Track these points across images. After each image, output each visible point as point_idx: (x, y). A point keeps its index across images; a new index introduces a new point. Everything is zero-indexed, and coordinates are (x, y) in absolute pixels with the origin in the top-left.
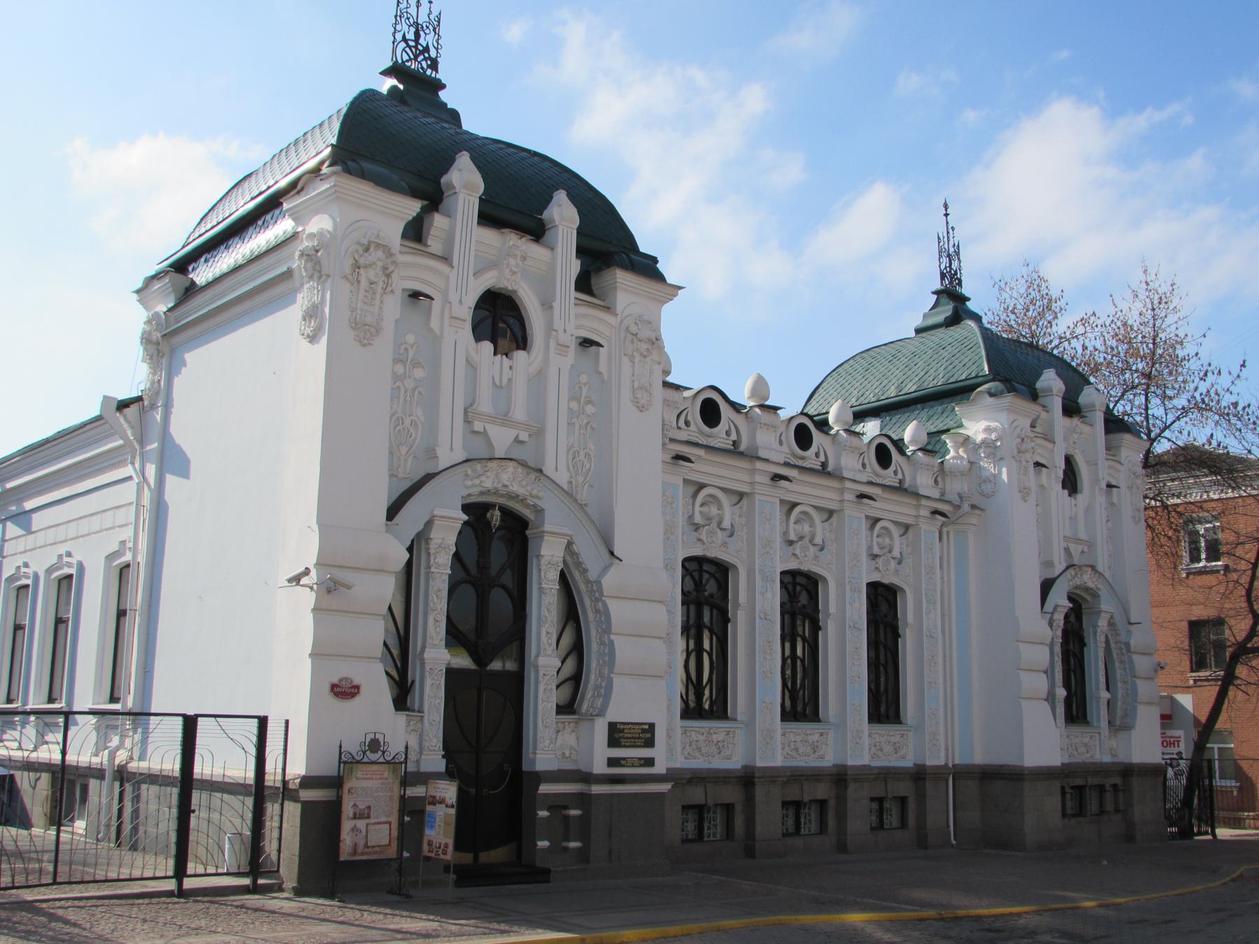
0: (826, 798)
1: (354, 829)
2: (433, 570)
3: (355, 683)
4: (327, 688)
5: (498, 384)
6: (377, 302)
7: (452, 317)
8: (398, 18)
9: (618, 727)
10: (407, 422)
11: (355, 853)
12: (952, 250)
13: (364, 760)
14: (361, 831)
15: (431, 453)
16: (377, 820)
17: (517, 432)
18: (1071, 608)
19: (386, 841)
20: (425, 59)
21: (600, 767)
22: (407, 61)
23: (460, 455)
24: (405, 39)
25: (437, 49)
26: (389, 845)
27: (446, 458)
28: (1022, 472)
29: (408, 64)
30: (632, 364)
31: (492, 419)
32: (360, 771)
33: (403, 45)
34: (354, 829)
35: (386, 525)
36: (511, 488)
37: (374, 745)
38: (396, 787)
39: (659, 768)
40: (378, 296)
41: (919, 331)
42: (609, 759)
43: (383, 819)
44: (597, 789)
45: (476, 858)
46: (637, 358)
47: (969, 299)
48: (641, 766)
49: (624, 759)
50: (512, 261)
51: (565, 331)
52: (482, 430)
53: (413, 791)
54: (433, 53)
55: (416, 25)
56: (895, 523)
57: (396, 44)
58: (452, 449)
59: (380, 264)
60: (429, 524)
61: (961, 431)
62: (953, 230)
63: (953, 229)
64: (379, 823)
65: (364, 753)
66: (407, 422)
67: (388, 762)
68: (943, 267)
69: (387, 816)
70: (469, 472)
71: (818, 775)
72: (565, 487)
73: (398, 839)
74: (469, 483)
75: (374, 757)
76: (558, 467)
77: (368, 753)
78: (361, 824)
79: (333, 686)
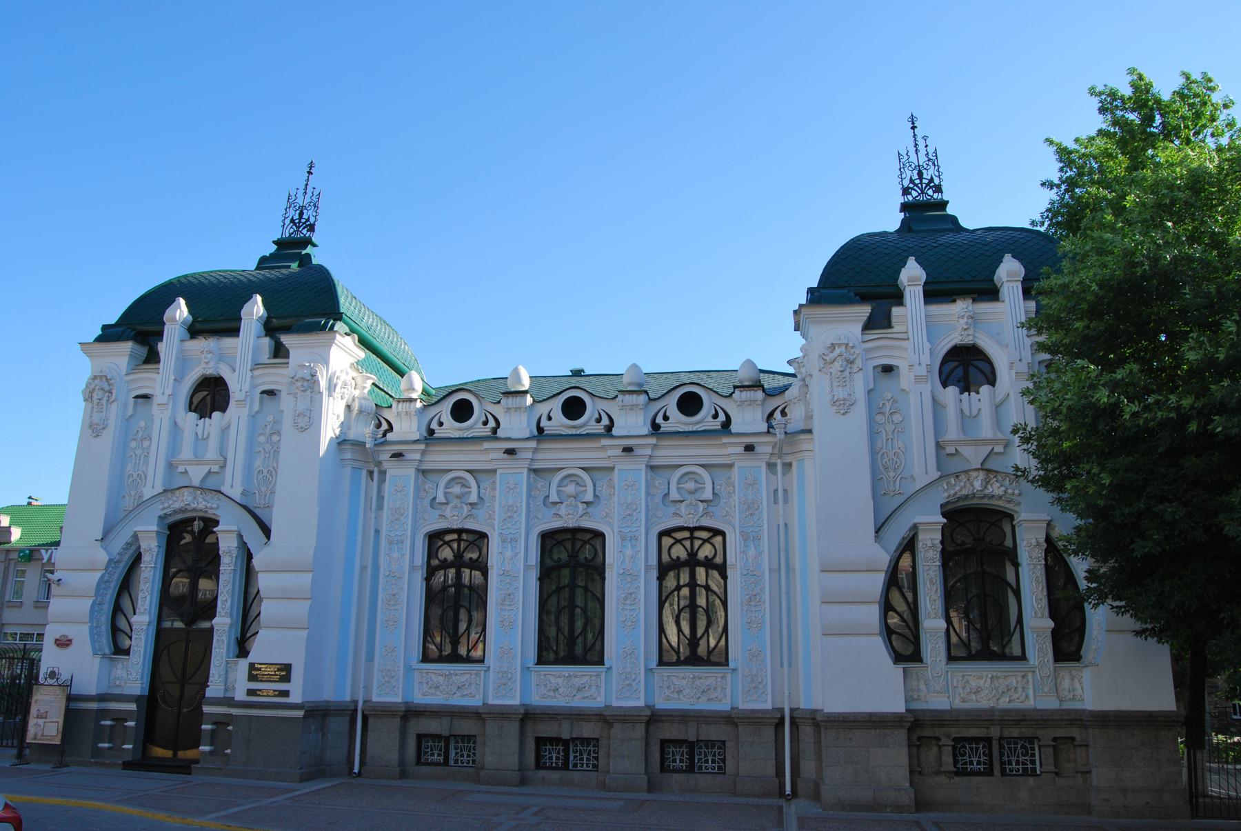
0: (596, 736)
1: (37, 724)
3: (69, 638)
4: (54, 641)
5: (200, 437)
6: (104, 409)
8: (288, 210)
9: (256, 666)
10: (135, 476)
11: (35, 739)
12: (923, 159)
14: (40, 726)
16: (51, 720)
18: (945, 524)
19: (55, 734)
21: (240, 695)
22: (292, 233)
24: (292, 221)
26: (56, 736)
27: (148, 493)
29: (293, 236)
30: (295, 399)
31: (189, 462)
33: (292, 224)
34: (37, 724)
36: (193, 505)
39: (295, 698)
40: (105, 406)
42: (248, 690)
44: (235, 711)
45: (175, 754)
48: (275, 696)
49: (260, 690)
52: (183, 471)
53: (74, 705)
54: (312, 220)
58: (153, 487)
60: (135, 537)
62: (925, 140)
63: (925, 138)
64: (52, 722)
65: (46, 679)
66: (135, 476)
67: (60, 685)
68: (906, 183)
69: (57, 718)
71: (580, 715)
72: (238, 498)
73: (62, 732)
74: (161, 507)
75: (51, 682)
77: (48, 679)
78: (41, 722)
79: (57, 640)
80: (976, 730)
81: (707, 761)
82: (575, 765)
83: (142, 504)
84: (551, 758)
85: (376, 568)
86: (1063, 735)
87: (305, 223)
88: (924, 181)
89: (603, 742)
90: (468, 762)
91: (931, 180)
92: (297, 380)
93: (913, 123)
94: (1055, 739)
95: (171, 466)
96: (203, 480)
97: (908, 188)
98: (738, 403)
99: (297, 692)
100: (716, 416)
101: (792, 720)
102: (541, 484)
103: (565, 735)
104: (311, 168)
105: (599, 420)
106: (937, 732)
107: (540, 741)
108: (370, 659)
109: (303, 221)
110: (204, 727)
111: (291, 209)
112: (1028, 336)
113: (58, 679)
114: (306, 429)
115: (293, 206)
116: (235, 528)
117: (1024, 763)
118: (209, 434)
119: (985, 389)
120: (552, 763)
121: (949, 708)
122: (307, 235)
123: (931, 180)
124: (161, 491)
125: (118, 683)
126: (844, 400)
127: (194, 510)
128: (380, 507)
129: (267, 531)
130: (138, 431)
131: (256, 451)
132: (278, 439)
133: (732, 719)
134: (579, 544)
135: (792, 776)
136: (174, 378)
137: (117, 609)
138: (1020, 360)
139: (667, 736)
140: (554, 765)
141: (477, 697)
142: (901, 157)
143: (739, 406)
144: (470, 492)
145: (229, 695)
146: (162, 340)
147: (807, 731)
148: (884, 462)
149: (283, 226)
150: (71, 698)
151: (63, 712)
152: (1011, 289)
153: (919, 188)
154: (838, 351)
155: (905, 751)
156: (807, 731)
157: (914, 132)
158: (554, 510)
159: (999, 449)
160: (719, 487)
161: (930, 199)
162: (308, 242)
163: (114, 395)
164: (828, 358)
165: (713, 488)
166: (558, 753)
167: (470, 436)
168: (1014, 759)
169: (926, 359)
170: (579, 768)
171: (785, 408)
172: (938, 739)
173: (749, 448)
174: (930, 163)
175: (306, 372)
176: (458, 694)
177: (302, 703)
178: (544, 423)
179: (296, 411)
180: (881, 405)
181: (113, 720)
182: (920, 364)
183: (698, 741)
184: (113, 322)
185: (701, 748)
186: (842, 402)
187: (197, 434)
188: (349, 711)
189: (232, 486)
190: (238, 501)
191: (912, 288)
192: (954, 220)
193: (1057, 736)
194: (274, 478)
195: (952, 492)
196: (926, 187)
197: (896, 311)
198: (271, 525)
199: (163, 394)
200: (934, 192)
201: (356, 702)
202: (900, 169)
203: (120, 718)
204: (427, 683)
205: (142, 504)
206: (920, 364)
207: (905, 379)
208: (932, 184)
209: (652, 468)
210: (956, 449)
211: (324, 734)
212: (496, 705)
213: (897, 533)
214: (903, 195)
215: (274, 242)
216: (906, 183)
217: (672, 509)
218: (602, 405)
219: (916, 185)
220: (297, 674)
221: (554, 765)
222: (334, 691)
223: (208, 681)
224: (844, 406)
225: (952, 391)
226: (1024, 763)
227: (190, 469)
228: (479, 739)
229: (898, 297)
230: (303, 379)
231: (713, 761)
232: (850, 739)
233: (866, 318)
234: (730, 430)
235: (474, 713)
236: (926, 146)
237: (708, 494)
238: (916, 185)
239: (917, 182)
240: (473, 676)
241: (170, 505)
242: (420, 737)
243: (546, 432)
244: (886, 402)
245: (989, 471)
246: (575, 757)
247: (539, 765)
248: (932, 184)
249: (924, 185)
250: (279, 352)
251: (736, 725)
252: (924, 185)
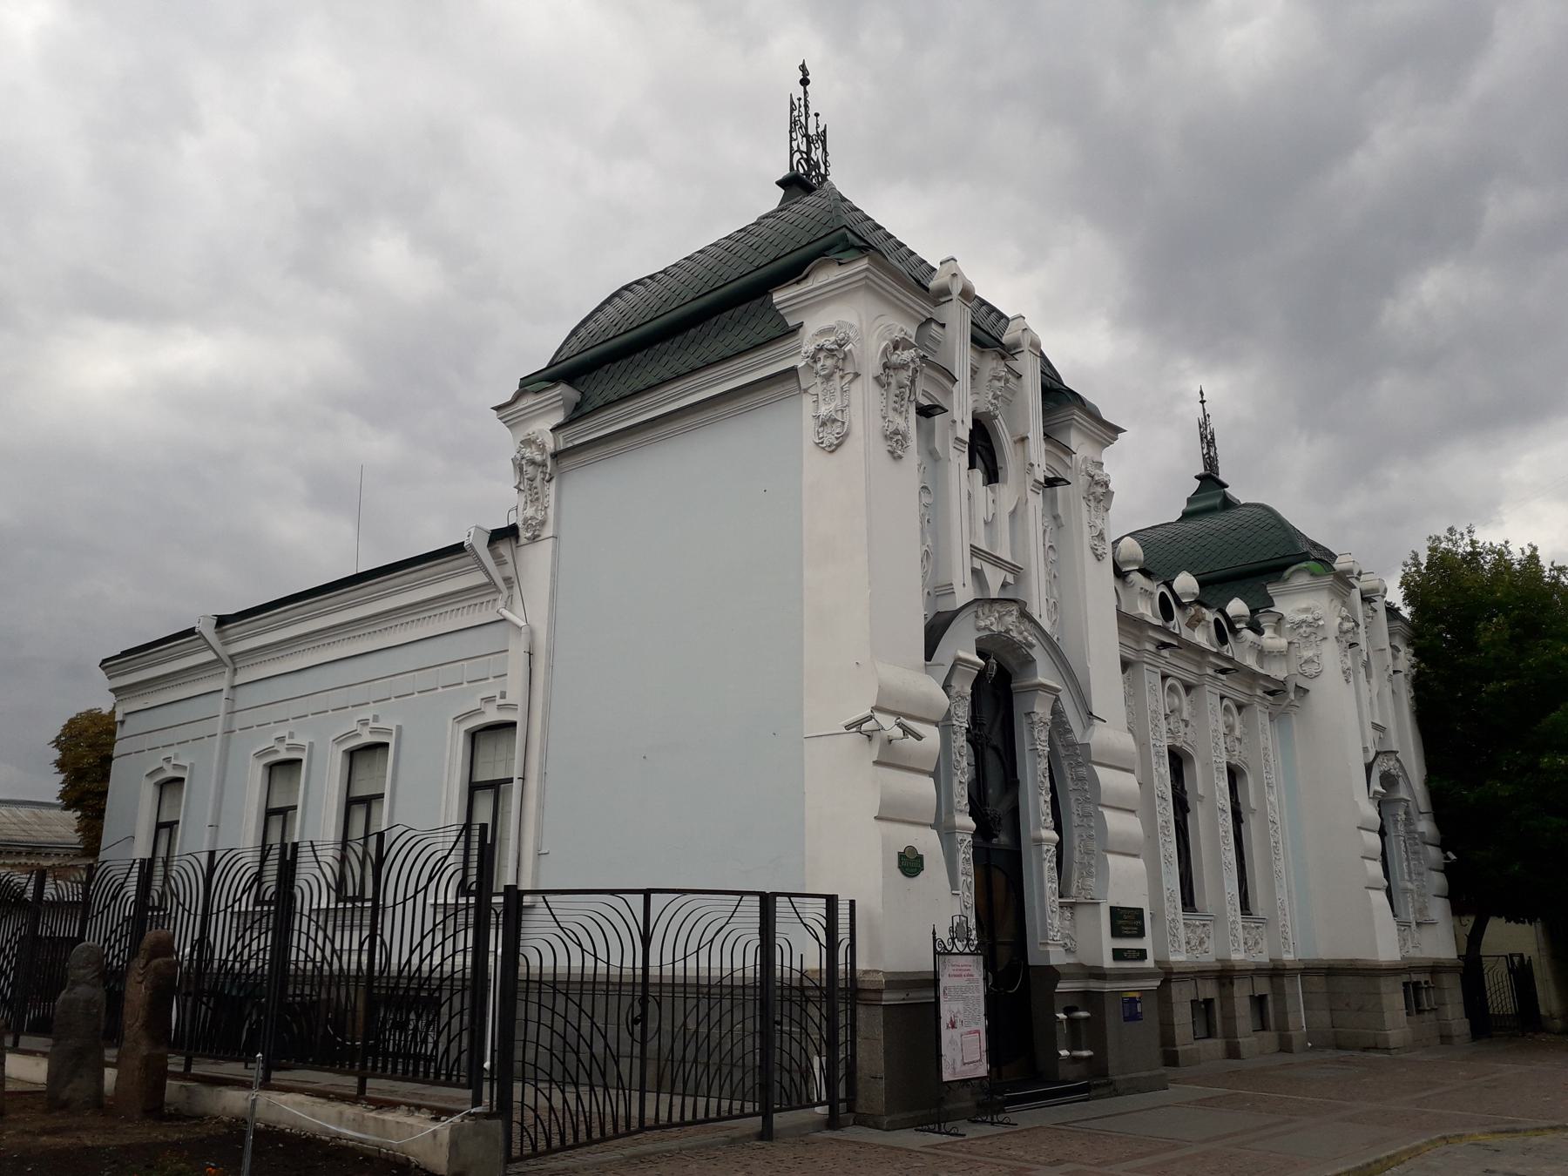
2: (955, 722)
7: (957, 439)
12: (1209, 437)
13: (955, 951)
15: (947, 590)
21: (1108, 962)
25: (825, 164)
26: (980, 1060)
35: (926, 665)
41: (1186, 515)
44: (1108, 986)
46: (1092, 504)
47: (1227, 486)
54: (823, 171)
55: (806, 135)
56: (1221, 704)
59: (912, 366)
61: (1271, 609)
63: (1208, 415)
70: (980, 613)
79: (901, 856)
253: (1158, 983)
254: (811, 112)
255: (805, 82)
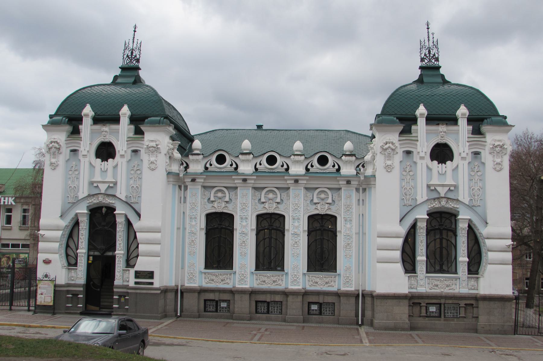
4: (42, 261)
5: (103, 170)
7: (83, 155)
12: (431, 44)
13: (44, 280)
17: (109, 184)
20: (135, 60)
21: (132, 284)
22: (128, 63)
23: (86, 194)
24: (128, 56)
26: (51, 302)
27: (81, 197)
28: (387, 159)
32: (42, 282)
33: (127, 58)
37: (46, 276)
38: (53, 287)
43: (49, 295)
44: (129, 291)
47: (440, 67)
50: (103, 133)
51: (122, 150)
52: (96, 185)
53: (57, 289)
54: (138, 57)
57: (124, 59)
58: (83, 193)
60: (77, 215)
63: (433, 34)
67: (50, 280)
68: (423, 56)
72: (124, 199)
74: (88, 202)
75: (46, 279)
76: (121, 192)
80: (435, 300)
81: (326, 311)
82: (272, 312)
83: (78, 201)
84: (261, 309)
85: (184, 229)
86: (468, 303)
87: (134, 58)
88: (431, 55)
89: (284, 303)
90: (226, 311)
91: (434, 55)
92: (150, 147)
93: (428, 26)
94: (465, 304)
95: (91, 183)
96: (106, 190)
97: (423, 58)
98: (344, 162)
99: (157, 283)
100: (334, 166)
101: (363, 295)
102: (257, 193)
103: (268, 300)
104: (135, 28)
105: (282, 166)
106: (420, 301)
107: (257, 302)
108: (183, 268)
109: (133, 56)
110: (114, 297)
111: (127, 50)
112: (468, 142)
113: (49, 278)
114: (155, 169)
115: (127, 48)
116: (124, 212)
117: (453, 313)
118: (107, 169)
119: (448, 163)
120: (262, 311)
121: (425, 292)
122: (136, 64)
123: (434, 55)
124: (87, 195)
125: (72, 279)
126: (390, 166)
127: (104, 203)
128: (185, 202)
129: (139, 215)
130: (72, 166)
131: (130, 177)
132: (140, 172)
133: (338, 295)
134: (273, 220)
135: (362, 317)
136: (89, 143)
137: (68, 246)
138: (464, 152)
139: (311, 300)
140: (263, 312)
141: (230, 284)
142: (421, 43)
143: (344, 163)
144: (226, 196)
145: (125, 283)
146: (82, 124)
147: (368, 300)
148: (405, 191)
149: (123, 59)
150: (55, 286)
151: (53, 292)
152: (462, 120)
153: (428, 58)
154: (388, 145)
155: (407, 308)
156: (368, 300)
157: (428, 31)
158: (263, 205)
159: (452, 188)
160: (335, 197)
161: (433, 64)
162: (138, 68)
163: (61, 150)
164: (384, 148)
165: (332, 198)
166: (264, 307)
167: (224, 171)
168: (449, 312)
169: (425, 150)
170: (273, 313)
171: (364, 164)
172: (420, 303)
173: (348, 182)
174: (434, 47)
175: (154, 144)
176: (222, 283)
177: (159, 287)
178: (258, 166)
179: (149, 161)
180: (405, 168)
181: (72, 295)
182: (422, 152)
183: (323, 302)
184: (53, 114)
185: (324, 305)
186: (389, 167)
187: (101, 169)
188: (175, 291)
189: (121, 193)
190: (124, 200)
191: (421, 119)
192: (443, 76)
193: (467, 303)
194: (139, 190)
195: (432, 206)
196: (431, 58)
197: (413, 127)
198: (140, 210)
199: (85, 150)
200: (435, 61)
201: (177, 286)
202: (420, 49)
203: (75, 295)
204: (208, 278)
205: (78, 201)
206: (422, 152)
207: (416, 157)
208: (434, 57)
209: (307, 189)
210: (435, 188)
211: (165, 300)
212: (239, 288)
213: (409, 222)
214: (421, 61)
215: (120, 68)
216: (423, 56)
217: (314, 206)
218: (284, 160)
219: (427, 57)
220: (156, 275)
221: (263, 312)
222: (171, 283)
223: (115, 278)
224: (389, 169)
225: (435, 162)
226: (453, 313)
227: (100, 185)
228: (231, 302)
229: (414, 120)
230: (153, 147)
231: (329, 311)
232: (386, 303)
233: (401, 131)
234: (340, 173)
235: (229, 291)
236: (433, 38)
237: (330, 201)
238: (427, 57)
239: (428, 55)
240: (228, 275)
241: (92, 201)
242: (205, 301)
243: (259, 170)
244: (407, 166)
245: (448, 198)
246: (271, 309)
247: (257, 312)
248: (434, 57)
249: (431, 57)
250: (139, 132)
251: (339, 296)
252: (431, 57)
253: (160, 292)
254: (135, 41)
255: (135, 31)
